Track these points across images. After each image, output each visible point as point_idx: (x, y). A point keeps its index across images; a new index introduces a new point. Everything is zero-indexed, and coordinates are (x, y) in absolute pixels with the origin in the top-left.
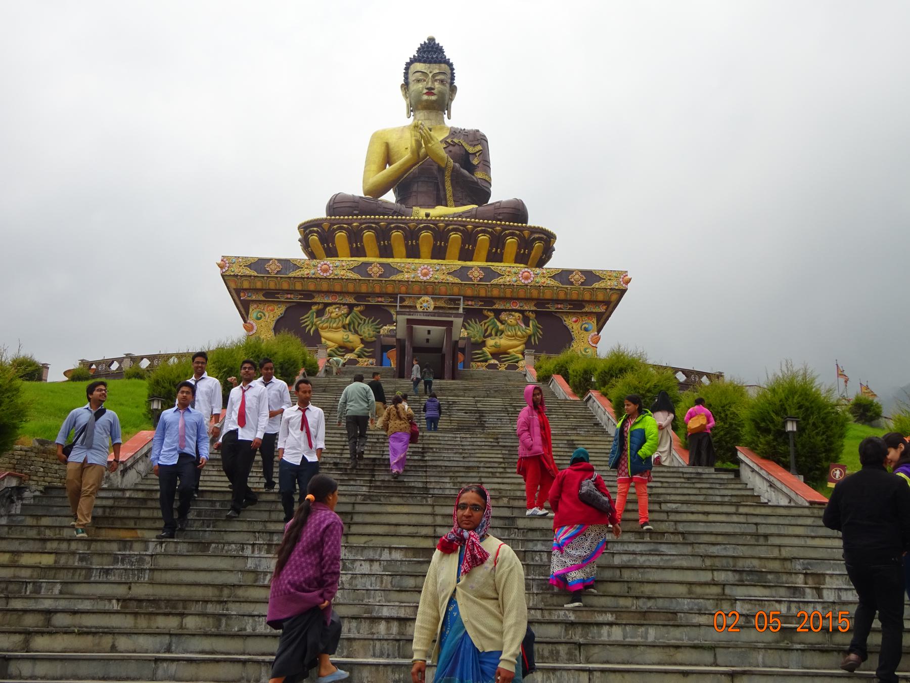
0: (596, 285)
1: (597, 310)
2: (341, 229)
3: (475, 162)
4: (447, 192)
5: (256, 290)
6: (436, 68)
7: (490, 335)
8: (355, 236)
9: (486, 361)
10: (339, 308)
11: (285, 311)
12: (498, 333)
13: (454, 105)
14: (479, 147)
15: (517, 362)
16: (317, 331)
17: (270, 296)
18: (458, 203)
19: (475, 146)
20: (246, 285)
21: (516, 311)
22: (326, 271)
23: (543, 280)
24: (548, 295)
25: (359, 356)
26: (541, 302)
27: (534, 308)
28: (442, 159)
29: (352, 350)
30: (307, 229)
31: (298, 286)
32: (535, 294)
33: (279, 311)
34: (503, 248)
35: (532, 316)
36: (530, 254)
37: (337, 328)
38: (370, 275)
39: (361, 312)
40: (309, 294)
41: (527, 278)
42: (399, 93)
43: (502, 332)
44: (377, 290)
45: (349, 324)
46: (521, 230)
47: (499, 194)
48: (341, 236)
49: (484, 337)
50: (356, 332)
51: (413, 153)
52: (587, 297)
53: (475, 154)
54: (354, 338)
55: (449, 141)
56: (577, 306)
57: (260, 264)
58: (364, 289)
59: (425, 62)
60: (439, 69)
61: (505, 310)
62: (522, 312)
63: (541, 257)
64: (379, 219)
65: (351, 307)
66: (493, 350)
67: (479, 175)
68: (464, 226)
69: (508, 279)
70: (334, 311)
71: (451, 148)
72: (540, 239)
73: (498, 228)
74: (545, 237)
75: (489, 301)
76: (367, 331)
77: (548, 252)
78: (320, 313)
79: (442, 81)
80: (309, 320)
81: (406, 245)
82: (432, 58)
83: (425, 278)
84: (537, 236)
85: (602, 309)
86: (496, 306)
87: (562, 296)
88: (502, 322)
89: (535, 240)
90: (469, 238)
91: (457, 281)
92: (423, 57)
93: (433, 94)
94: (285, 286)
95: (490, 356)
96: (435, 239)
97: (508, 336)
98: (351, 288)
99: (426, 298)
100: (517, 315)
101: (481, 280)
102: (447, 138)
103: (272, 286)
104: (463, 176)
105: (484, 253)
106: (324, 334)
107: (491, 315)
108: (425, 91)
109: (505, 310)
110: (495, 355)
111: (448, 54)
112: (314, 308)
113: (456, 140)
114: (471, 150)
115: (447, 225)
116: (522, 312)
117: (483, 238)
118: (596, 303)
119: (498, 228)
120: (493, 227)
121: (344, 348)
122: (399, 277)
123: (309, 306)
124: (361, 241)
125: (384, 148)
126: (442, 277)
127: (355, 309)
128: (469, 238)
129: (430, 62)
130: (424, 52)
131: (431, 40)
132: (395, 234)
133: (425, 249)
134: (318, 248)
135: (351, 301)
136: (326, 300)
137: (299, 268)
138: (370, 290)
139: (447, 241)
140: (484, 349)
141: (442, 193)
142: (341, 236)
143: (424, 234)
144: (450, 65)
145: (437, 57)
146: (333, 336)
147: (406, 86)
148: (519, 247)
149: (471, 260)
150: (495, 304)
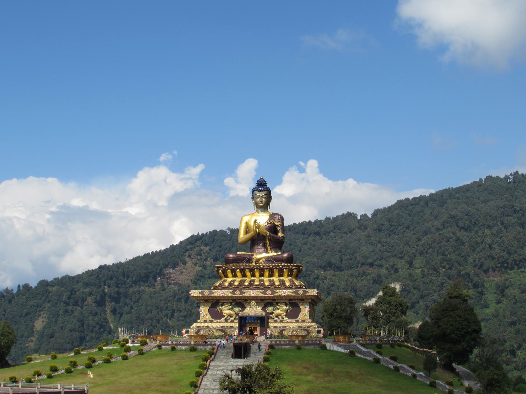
0: (307, 294)
1: (308, 301)
2: (229, 269)
3: (278, 229)
4: (268, 244)
5: (202, 300)
6: (263, 194)
7: (275, 310)
8: (234, 272)
9: (274, 319)
10: (228, 303)
11: (212, 305)
12: (278, 309)
14: (280, 223)
15: (284, 319)
16: (221, 311)
19: (278, 222)
20: (199, 299)
21: (283, 302)
22: (223, 294)
23: (290, 293)
24: (292, 298)
25: (235, 319)
26: (290, 300)
27: (288, 301)
28: (265, 233)
29: (232, 317)
31: (215, 298)
32: (288, 298)
33: (210, 304)
34: (283, 273)
35: (288, 303)
36: (292, 274)
37: (227, 310)
38: (236, 295)
39: (235, 304)
40: (218, 300)
41: (285, 293)
42: (251, 200)
43: (279, 309)
44: (239, 298)
45: (231, 309)
46: (289, 266)
49: (273, 310)
50: (233, 311)
51: (254, 232)
52: (304, 298)
53: (278, 225)
55: (268, 222)
58: (235, 298)
59: (259, 191)
60: (264, 193)
61: (279, 302)
62: (285, 303)
63: (297, 274)
64: (241, 266)
65: (231, 303)
66: (276, 315)
67: (280, 234)
68: (269, 267)
71: (269, 225)
72: (295, 269)
73: (281, 267)
74: (297, 268)
75: (274, 300)
79: (265, 198)
81: (251, 274)
82: (261, 189)
83: (253, 295)
84: (294, 268)
85: (310, 301)
86: (277, 301)
87: (296, 298)
88: (279, 306)
89: (294, 269)
91: (263, 295)
92: (258, 189)
93: (261, 203)
94: (211, 298)
95: (275, 317)
96: (260, 272)
97: (281, 310)
98: (231, 298)
99: (253, 302)
100: (283, 303)
101: (270, 294)
102: (268, 220)
103: (207, 299)
104: (273, 237)
105: (277, 274)
106: (224, 312)
107: (275, 304)
108: (259, 202)
109: (279, 302)
110: (277, 316)
111: (268, 185)
112: (220, 304)
113: (271, 221)
114: (277, 224)
115: (263, 267)
116: (285, 303)
118: (308, 299)
119: (281, 267)
120: (279, 266)
121: (231, 316)
122: (245, 295)
123: (219, 303)
124: (236, 273)
125: (245, 224)
126: (258, 294)
127: (233, 304)
129: (261, 191)
130: (259, 185)
131: (262, 178)
132: (247, 270)
133: (257, 274)
134: (222, 275)
135: (231, 301)
136: (224, 301)
137: (214, 293)
138: (237, 299)
139: (264, 272)
140: (274, 315)
141: (266, 244)
143: (256, 270)
145: (263, 189)
147: (253, 198)
148: (288, 272)
149: (273, 277)
150: (276, 300)
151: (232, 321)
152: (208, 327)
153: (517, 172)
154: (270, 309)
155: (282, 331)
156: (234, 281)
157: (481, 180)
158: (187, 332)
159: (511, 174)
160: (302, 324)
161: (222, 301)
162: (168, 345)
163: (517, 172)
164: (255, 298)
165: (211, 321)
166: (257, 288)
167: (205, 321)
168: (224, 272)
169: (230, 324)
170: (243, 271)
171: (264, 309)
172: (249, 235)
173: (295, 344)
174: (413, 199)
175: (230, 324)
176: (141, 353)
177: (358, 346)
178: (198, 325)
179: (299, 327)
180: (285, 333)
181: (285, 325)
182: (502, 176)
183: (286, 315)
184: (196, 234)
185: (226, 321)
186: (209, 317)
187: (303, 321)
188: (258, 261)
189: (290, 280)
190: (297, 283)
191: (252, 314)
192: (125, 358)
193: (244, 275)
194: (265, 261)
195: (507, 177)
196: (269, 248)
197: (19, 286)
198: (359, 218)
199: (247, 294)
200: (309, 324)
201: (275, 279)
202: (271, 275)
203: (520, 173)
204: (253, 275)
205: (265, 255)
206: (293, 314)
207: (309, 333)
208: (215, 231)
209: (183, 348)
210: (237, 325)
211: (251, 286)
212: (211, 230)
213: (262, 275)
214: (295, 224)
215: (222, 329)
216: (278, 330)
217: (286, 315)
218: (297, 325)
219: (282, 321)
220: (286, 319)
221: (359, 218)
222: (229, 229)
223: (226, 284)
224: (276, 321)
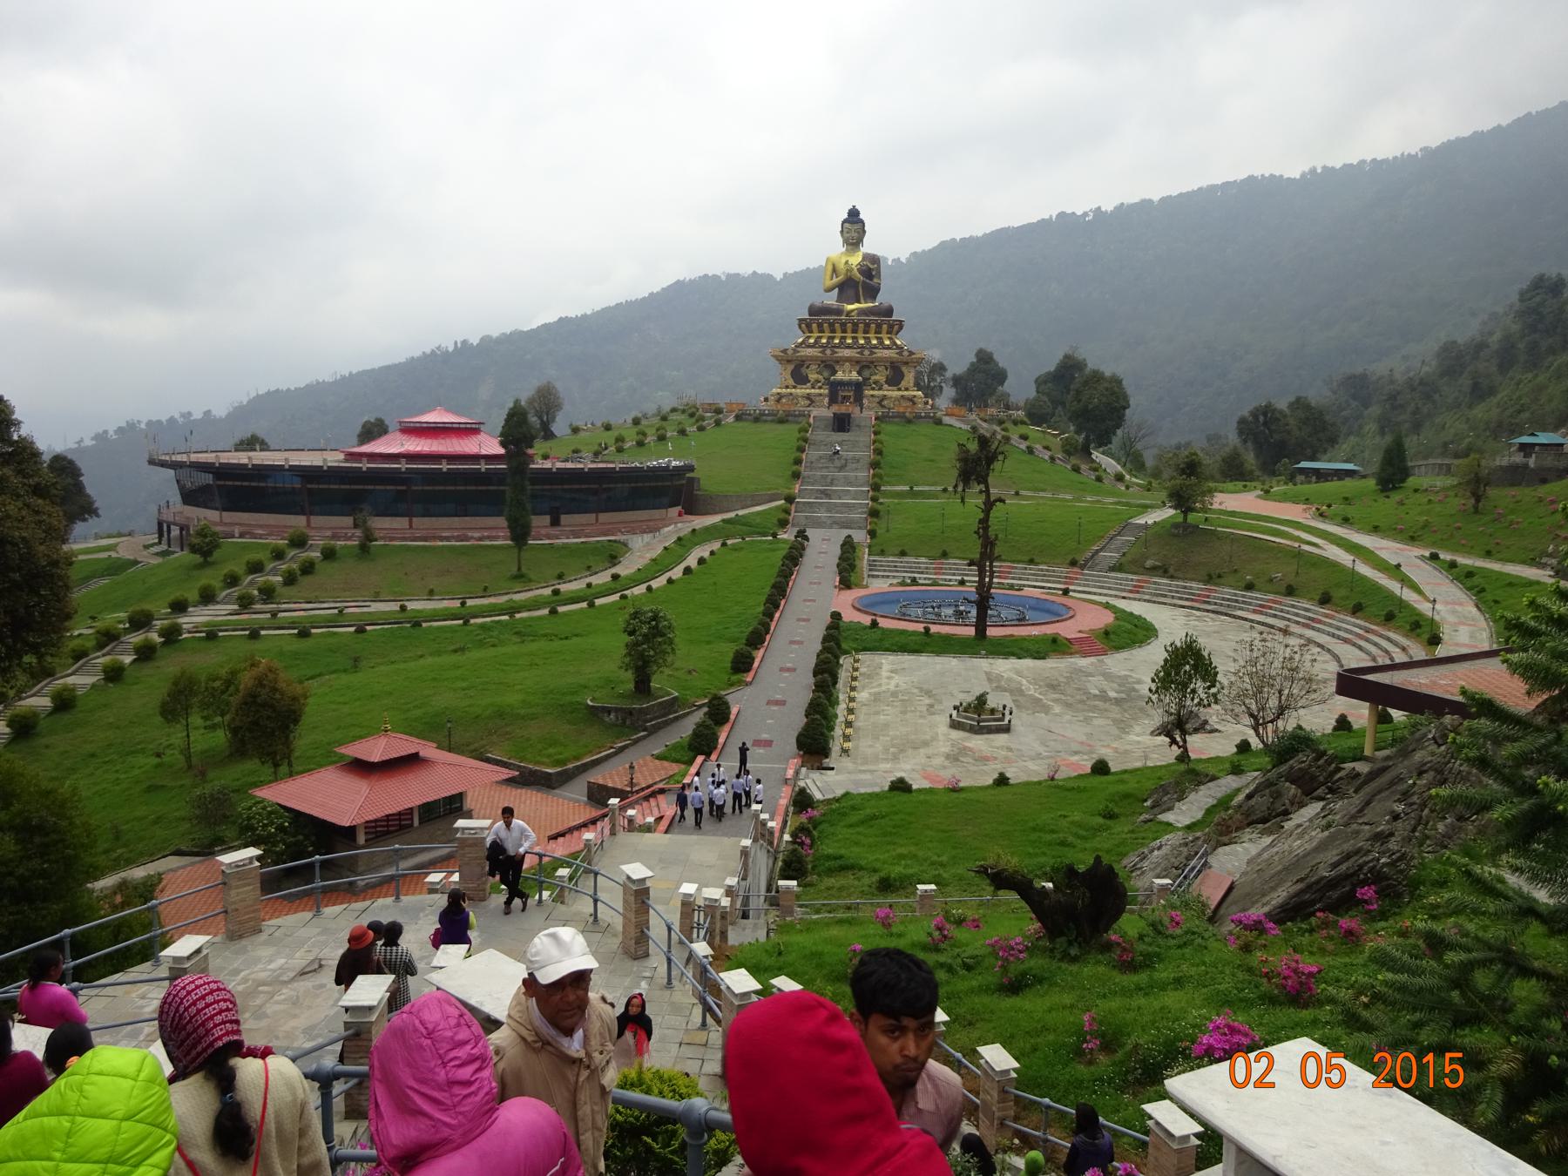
6: (856, 226)
8: (820, 326)
12: (876, 374)
13: (865, 240)
17: (789, 361)
18: (866, 303)
26: (892, 363)
30: (801, 321)
47: (882, 299)
48: (814, 326)
54: (820, 377)
56: (906, 363)
57: (785, 351)
67: (875, 280)
69: (879, 355)
70: (813, 367)
75: (872, 362)
76: (826, 374)
77: (901, 327)
78: (808, 367)
80: (803, 370)
90: (867, 325)
111: (861, 216)
114: (871, 267)
117: (873, 326)
128: (867, 325)
133: (849, 330)
134: (806, 330)
142: (814, 326)
144: (862, 222)
146: (813, 376)
147: (842, 232)
151: (820, 388)
152: (791, 394)
153: (1099, 208)
154: (866, 373)
155: (882, 400)
156: (821, 337)
157: (1051, 216)
158: (766, 400)
159: (1091, 210)
160: (906, 393)
161: (808, 363)
162: (750, 415)
163: (1099, 208)
164: (849, 360)
165: (795, 387)
166: (849, 347)
167: (787, 387)
168: (809, 326)
169: (817, 391)
170: (832, 325)
171: (859, 373)
172: (835, 280)
173: (906, 417)
174: (961, 239)
175: (817, 391)
176: (718, 423)
177: (979, 421)
178: (779, 390)
179: (902, 396)
180: (885, 403)
181: (885, 393)
182: (1079, 213)
183: (886, 382)
184: (682, 279)
185: (813, 388)
186: (791, 382)
187: (907, 389)
188: (849, 313)
189: (890, 339)
190: (898, 342)
191: (846, 378)
192: (701, 429)
193: (833, 331)
194: (859, 315)
195: (1085, 214)
196: (862, 300)
197: (456, 343)
198: (890, 263)
199: (840, 355)
200: (915, 393)
201: (871, 335)
202: (866, 332)
203: (1103, 209)
204: (844, 331)
205: (856, 306)
206: (895, 379)
207: (914, 403)
208: (706, 275)
209: (770, 418)
210: (827, 391)
211: (842, 345)
212: (701, 275)
213: (855, 331)
214: (808, 268)
215: (808, 397)
216: (877, 400)
217: (886, 382)
218: (901, 393)
219: (880, 389)
220: (886, 386)
221: (890, 263)
222: (724, 273)
223: (812, 341)
224: (873, 389)
